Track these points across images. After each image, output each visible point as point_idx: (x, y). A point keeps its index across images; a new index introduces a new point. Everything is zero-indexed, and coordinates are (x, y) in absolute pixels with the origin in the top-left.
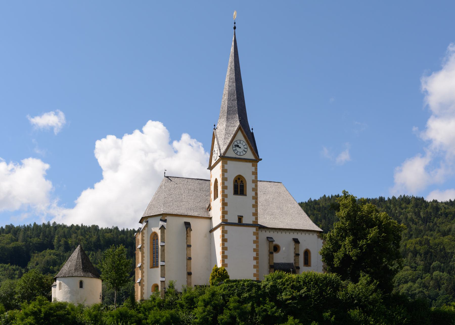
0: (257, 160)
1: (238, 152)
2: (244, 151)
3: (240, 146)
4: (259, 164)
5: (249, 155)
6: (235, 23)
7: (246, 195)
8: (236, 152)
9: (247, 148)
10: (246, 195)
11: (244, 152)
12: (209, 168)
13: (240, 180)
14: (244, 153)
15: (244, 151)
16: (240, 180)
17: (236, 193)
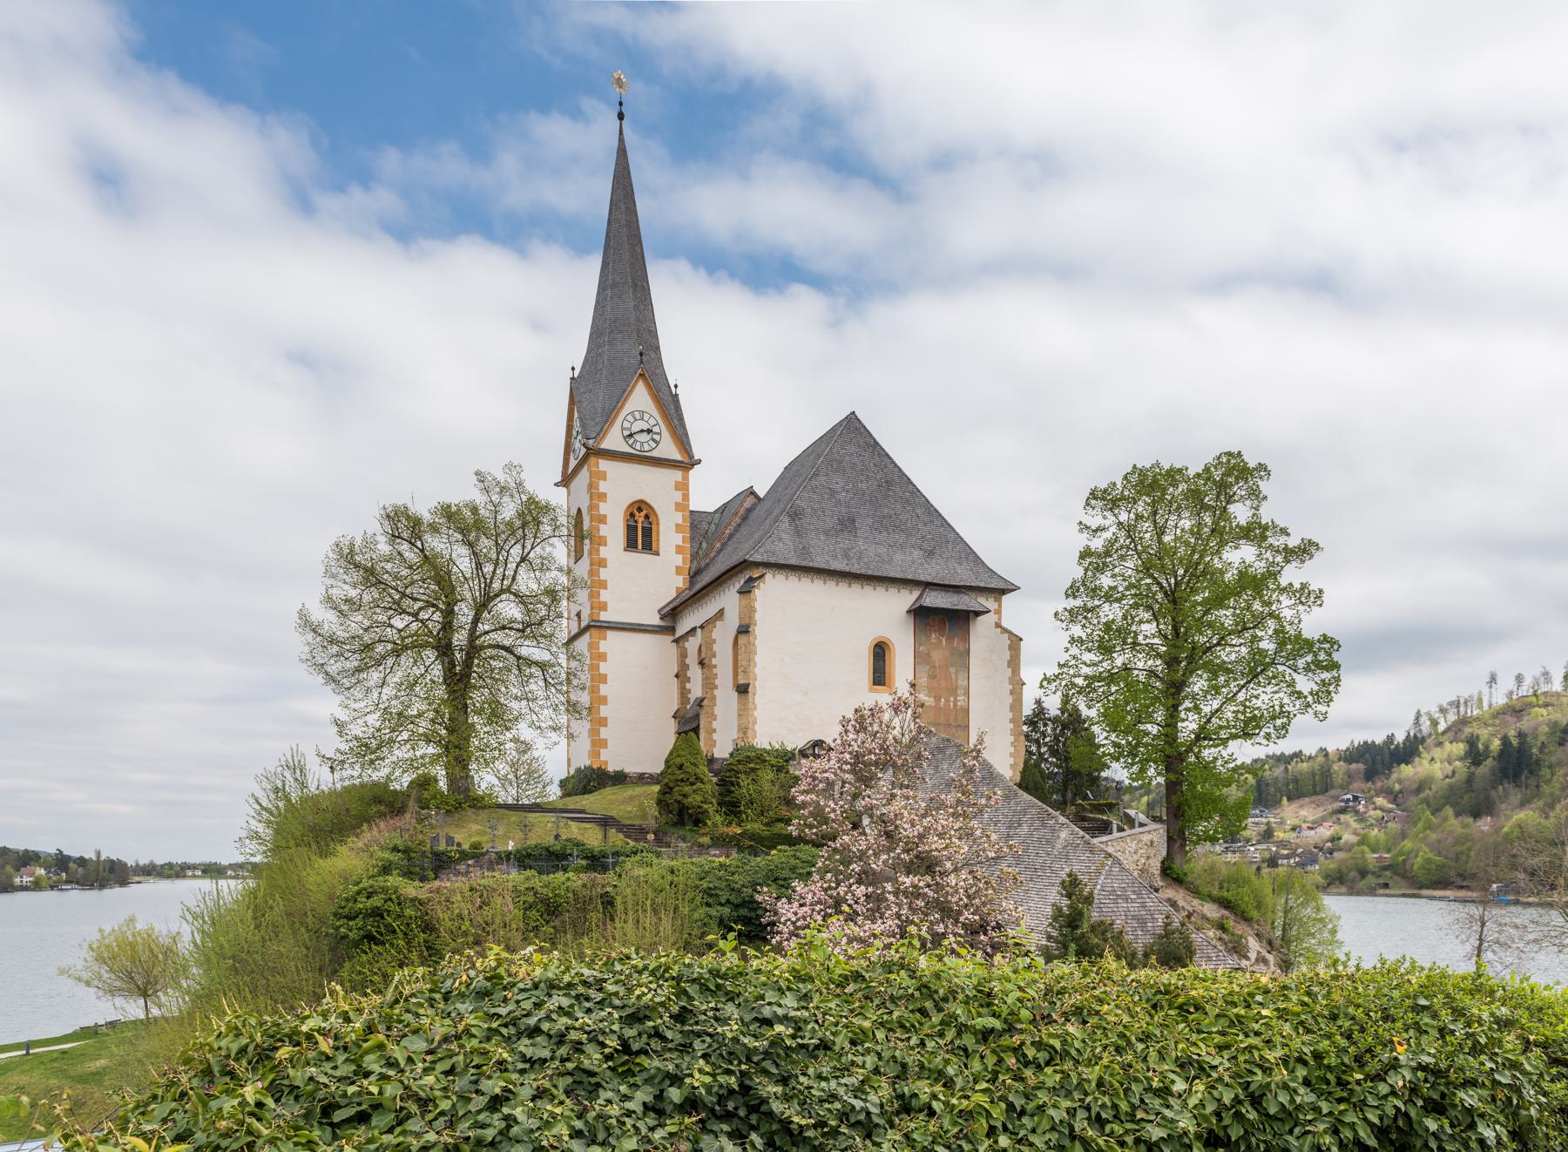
0: (687, 463)
1: (642, 443)
2: (653, 440)
3: (645, 434)
4: (694, 473)
5: (669, 449)
6: (621, 104)
7: (657, 554)
8: (630, 442)
9: (660, 434)
10: (657, 554)
11: (651, 443)
12: (562, 481)
13: (643, 514)
14: (654, 445)
15: (653, 440)
16: (643, 514)
17: (631, 544)
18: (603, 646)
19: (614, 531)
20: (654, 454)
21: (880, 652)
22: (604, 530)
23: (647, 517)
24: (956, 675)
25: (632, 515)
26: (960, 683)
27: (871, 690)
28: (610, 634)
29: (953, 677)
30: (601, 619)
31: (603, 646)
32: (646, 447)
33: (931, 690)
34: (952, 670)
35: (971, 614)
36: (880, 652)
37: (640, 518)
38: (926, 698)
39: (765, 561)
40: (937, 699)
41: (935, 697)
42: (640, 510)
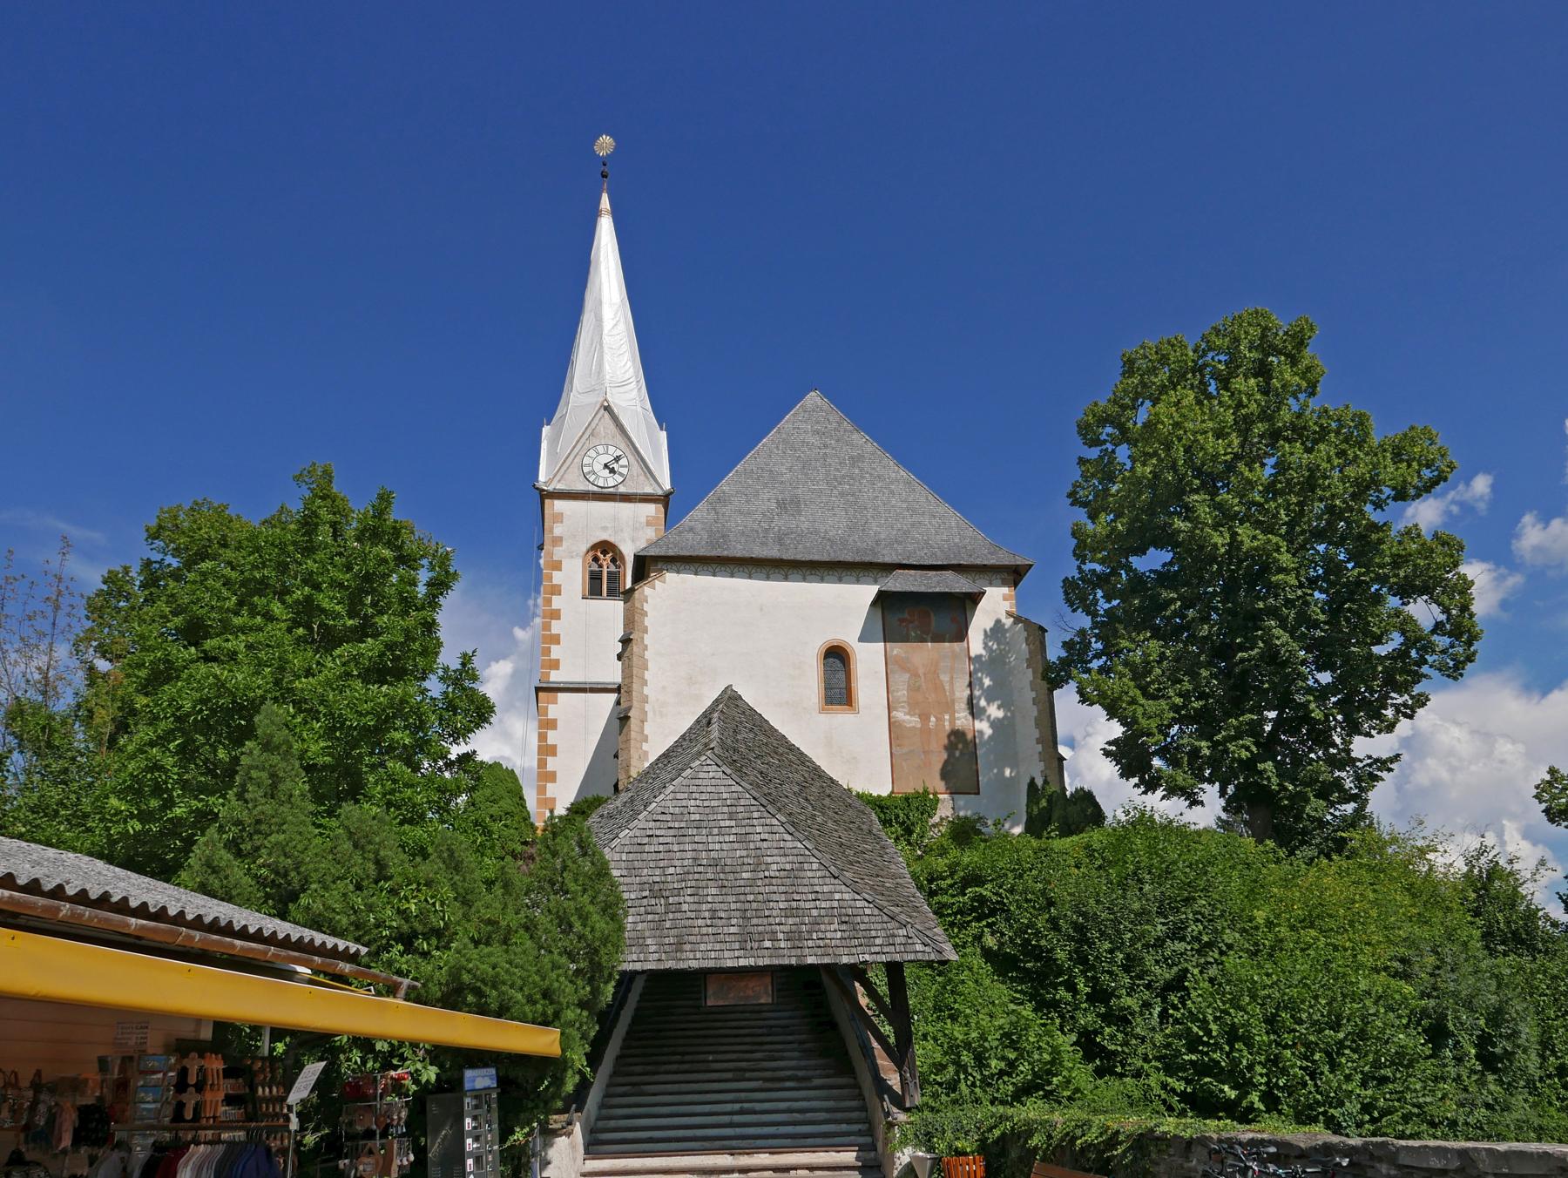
13: (609, 556)
15: (620, 474)
16: (609, 556)
17: (593, 587)
18: (553, 711)
19: (571, 574)
20: (622, 489)
21: (836, 656)
22: (557, 577)
23: (613, 560)
24: (952, 684)
25: (596, 559)
26: (957, 694)
27: (822, 711)
28: (560, 695)
29: (947, 688)
30: (551, 680)
31: (553, 711)
32: (611, 483)
33: (913, 706)
34: (945, 678)
35: (968, 602)
36: (836, 656)
37: (606, 560)
38: (908, 717)
39: (662, 554)
40: (925, 717)
41: (920, 716)
42: (605, 553)
